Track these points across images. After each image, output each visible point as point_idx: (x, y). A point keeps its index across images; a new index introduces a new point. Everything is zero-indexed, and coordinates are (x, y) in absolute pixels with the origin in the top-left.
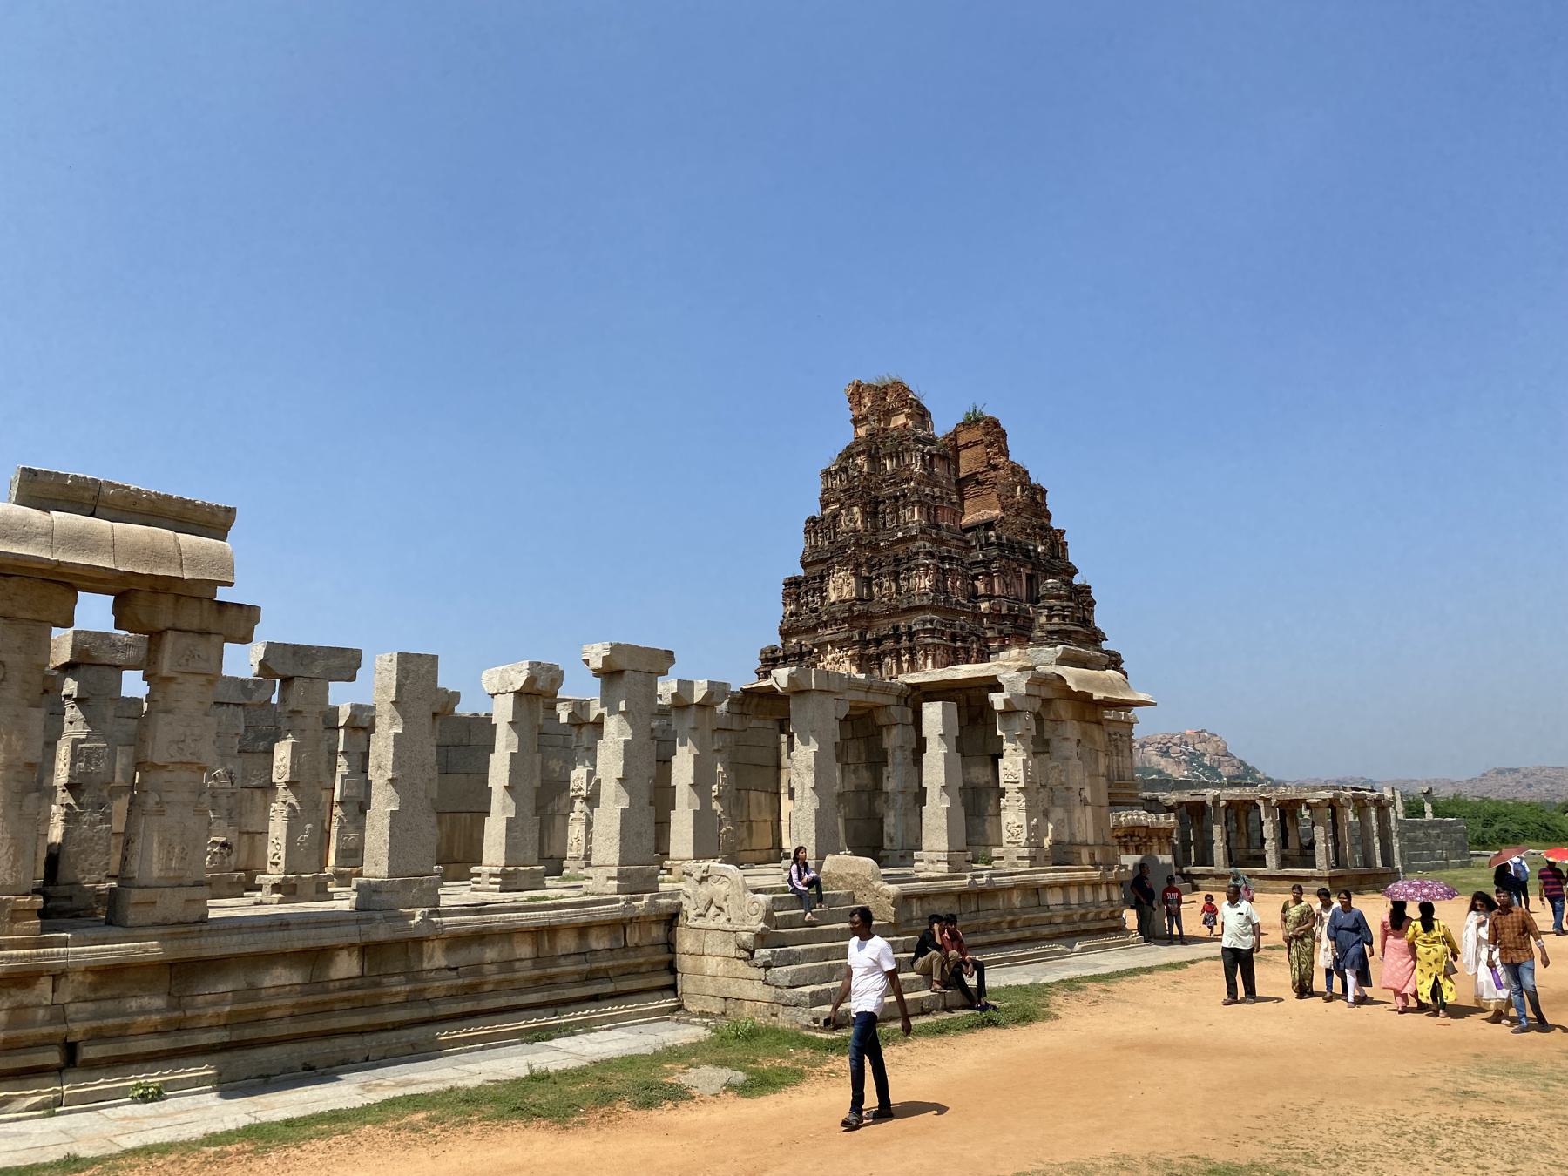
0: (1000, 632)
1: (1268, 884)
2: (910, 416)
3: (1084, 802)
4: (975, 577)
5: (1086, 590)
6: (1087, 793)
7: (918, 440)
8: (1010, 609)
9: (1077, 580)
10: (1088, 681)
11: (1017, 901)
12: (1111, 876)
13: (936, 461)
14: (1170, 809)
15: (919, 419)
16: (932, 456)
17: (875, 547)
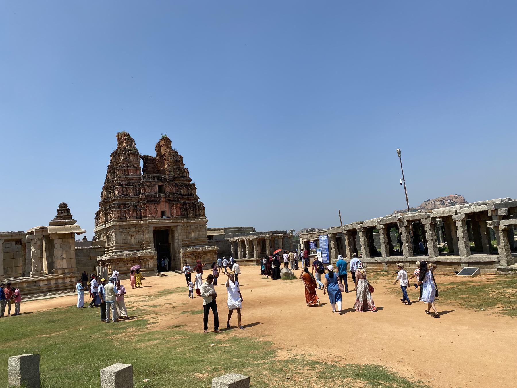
0: (143, 203)
1: (247, 263)
2: (126, 143)
3: (63, 258)
4: (140, 189)
5: (194, 185)
6: (64, 256)
7: (125, 150)
8: (148, 196)
9: (191, 183)
10: (56, 229)
11: (25, 285)
12: (69, 276)
14: (231, 243)
15: (130, 143)
16: (129, 155)
17: (113, 182)
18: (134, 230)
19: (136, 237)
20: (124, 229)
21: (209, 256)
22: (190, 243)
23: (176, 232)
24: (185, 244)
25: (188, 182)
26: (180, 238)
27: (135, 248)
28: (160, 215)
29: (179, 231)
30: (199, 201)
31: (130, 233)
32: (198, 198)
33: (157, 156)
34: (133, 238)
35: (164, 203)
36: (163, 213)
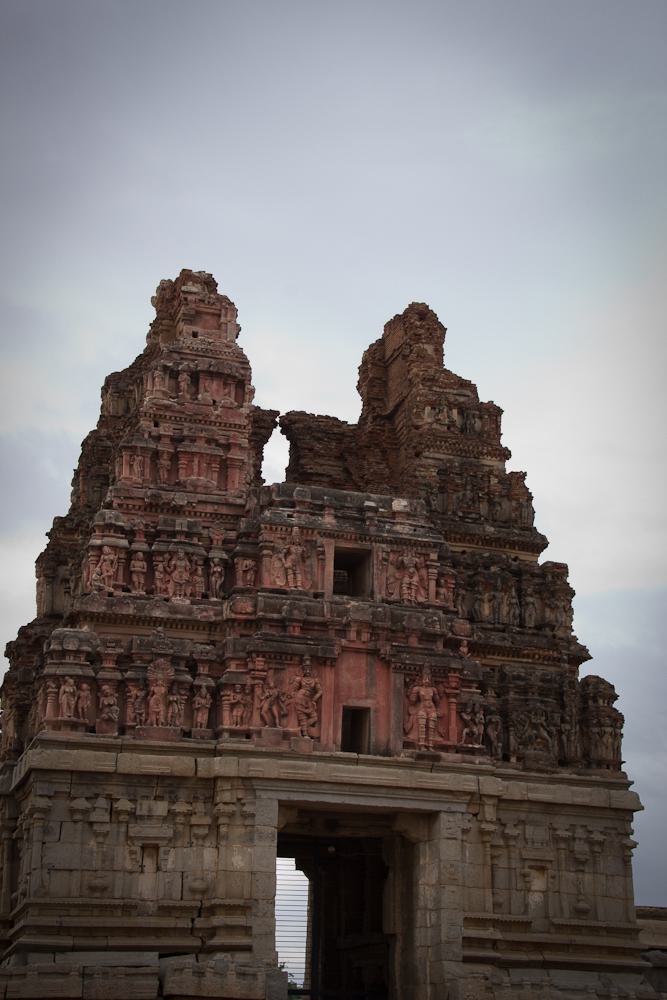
5: (560, 570)
9: (543, 558)
13: (204, 383)
18: (161, 808)
19: (171, 860)
20: (102, 802)
22: (517, 945)
23: (425, 860)
24: (481, 942)
25: (525, 556)
26: (451, 896)
27: (158, 931)
28: (332, 731)
29: (449, 850)
30: (585, 670)
31: (134, 830)
32: (583, 655)
33: (363, 419)
34: (149, 863)
35: (363, 661)
36: (355, 723)
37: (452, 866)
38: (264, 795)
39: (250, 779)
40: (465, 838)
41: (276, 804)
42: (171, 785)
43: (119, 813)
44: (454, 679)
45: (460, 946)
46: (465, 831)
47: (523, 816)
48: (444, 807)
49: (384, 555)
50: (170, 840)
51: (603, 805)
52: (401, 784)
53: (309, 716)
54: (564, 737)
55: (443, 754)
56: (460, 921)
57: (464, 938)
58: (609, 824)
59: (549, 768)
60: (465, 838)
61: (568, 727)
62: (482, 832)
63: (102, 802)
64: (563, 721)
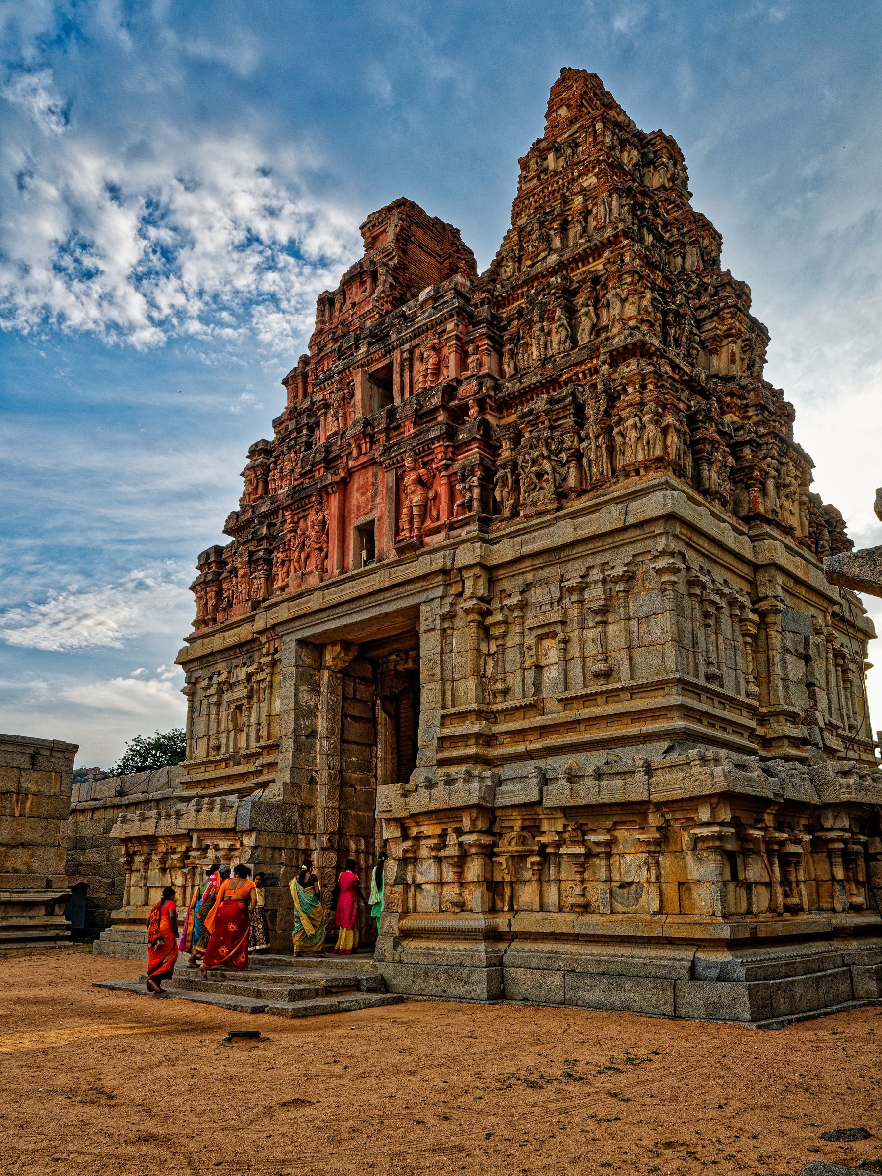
21: (631, 863)
37: (430, 661)
38: (287, 639)
39: (274, 627)
40: (447, 625)
41: (294, 643)
42: (248, 652)
43: (224, 683)
44: (439, 450)
45: (434, 749)
46: (443, 618)
47: (529, 577)
48: (423, 597)
49: (406, 355)
50: (250, 697)
51: (615, 526)
52: (377, 587)
53: (321, 549)
54: (584, 460)
55: (427, 539)
56: (437, 721)
57: (442, 740)
58: (639, 548)
59: (550, 507)
60: (447, 625)
61: (585, 444)
62: (467, 611)
63: (215, 679)
64: (581, 440)
